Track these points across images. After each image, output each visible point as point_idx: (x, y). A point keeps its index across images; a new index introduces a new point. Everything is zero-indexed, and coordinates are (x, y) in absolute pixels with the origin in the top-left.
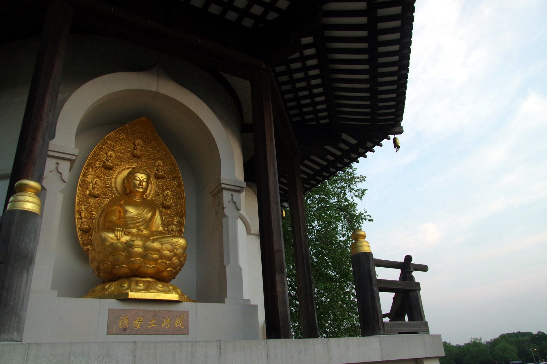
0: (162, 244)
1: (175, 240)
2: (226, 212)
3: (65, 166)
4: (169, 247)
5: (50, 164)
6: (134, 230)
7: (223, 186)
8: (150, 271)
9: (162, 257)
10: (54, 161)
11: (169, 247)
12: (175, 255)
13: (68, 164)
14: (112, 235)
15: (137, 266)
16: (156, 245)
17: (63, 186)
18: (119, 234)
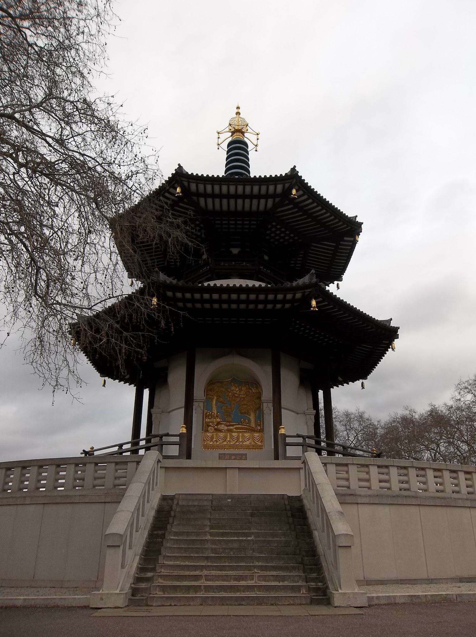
3: (201, 404)
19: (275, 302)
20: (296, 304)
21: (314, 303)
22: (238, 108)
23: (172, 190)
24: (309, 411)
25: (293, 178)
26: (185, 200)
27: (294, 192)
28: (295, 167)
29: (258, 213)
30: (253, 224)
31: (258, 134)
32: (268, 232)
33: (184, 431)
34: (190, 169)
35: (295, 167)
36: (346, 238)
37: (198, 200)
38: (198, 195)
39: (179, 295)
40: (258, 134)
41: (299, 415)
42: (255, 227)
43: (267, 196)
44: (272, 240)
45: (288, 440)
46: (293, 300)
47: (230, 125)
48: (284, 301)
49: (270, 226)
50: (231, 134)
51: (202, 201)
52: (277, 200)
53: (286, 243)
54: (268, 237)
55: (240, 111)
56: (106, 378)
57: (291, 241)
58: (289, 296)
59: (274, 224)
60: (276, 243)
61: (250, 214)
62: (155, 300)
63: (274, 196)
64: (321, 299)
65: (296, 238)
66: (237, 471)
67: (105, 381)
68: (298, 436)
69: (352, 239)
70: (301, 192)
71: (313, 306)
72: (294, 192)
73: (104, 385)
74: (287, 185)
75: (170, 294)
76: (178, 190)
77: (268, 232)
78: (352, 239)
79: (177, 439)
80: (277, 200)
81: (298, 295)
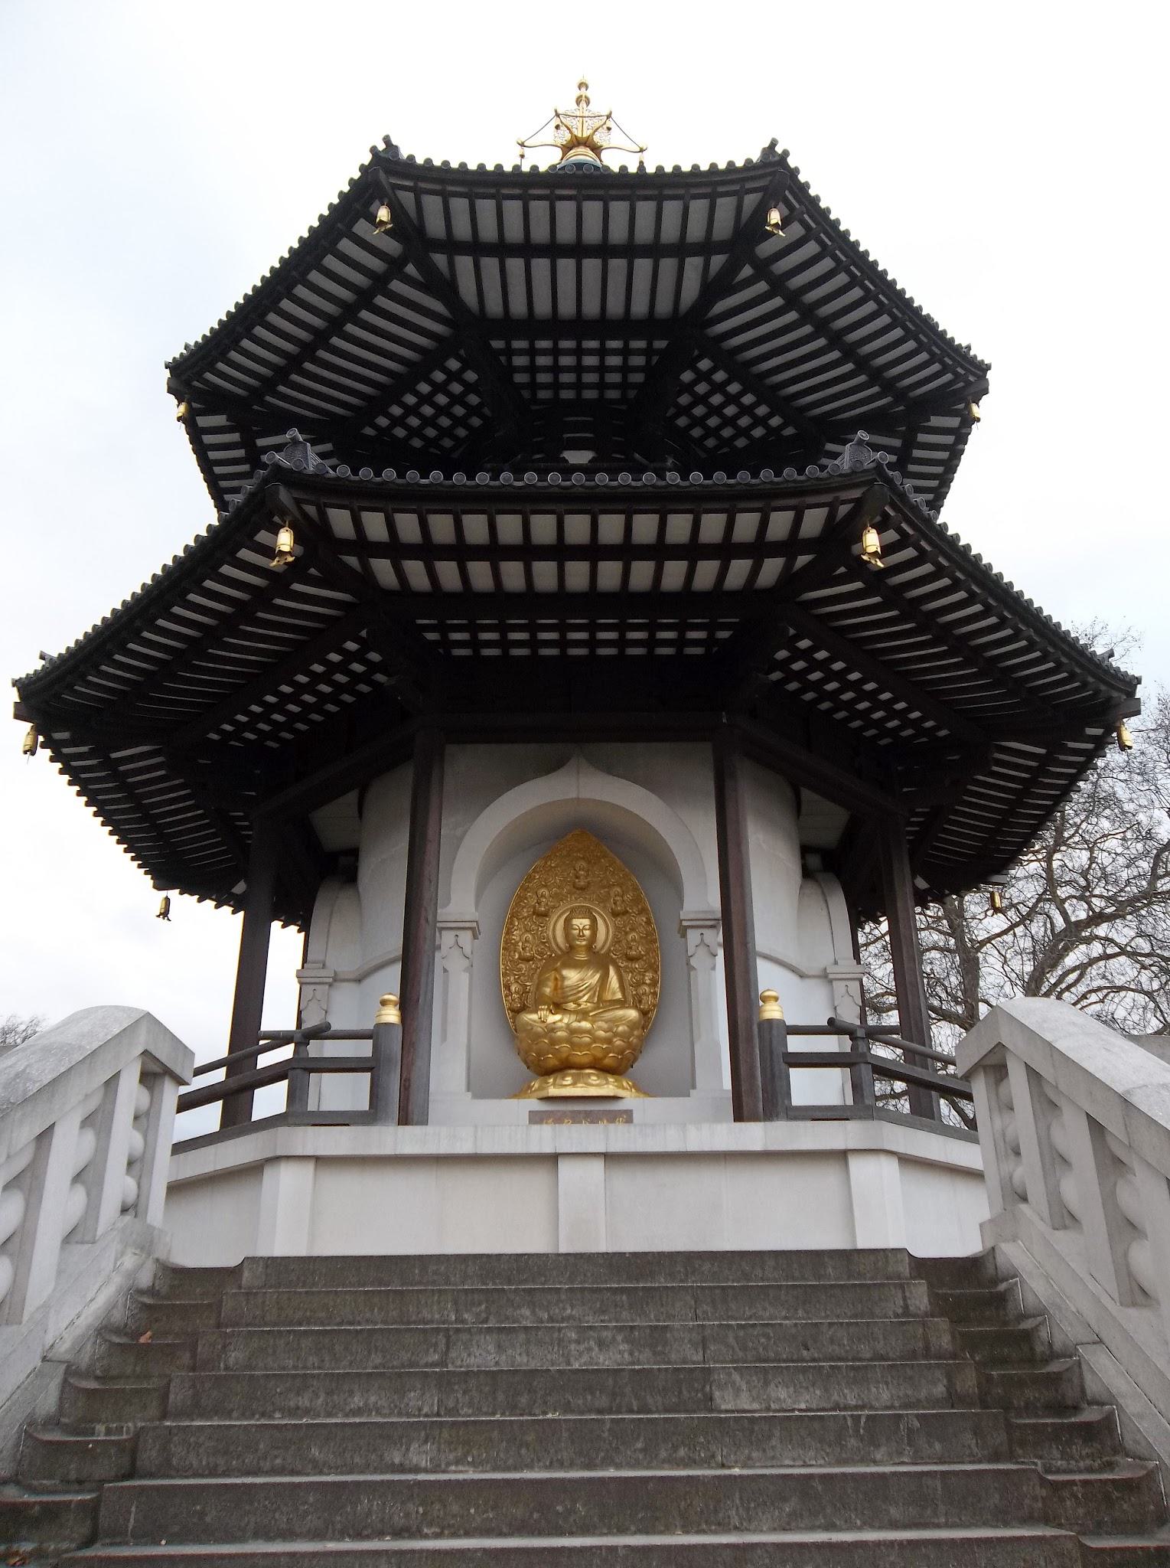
0: (593, 1022)
1: (620, 1013)
2: (693, 962)
3: (466, 938)
4: (605, 1026)
5: (447, 939)
6: (571, 1006)
7: (685, 923)
8: (585, 1060)
9: (595, 1039)
10: (453, 933)
11: (605, 1026)
12: (616, 1034)
13: (469, 933)
14: (534, 1017)
15: (564, 1055)
16: (585, 1025)
17: (466, 963)
18: (542, 1013)
19: (726, 550)
20: (802, 560)
21: (872, 540)
22: (582, 85)
23: (361, 227)
24: (836, 969)
25: (773, 177)
26: (410, 269)
27: (775, 217)
28: (774, 143)
29: (650, 326)
30: (636, 369)
31: (642, 150)
32: (684, 400)
33: (392, 1015)
34: (423, 146)
35: (774, 143)
36: (936, 421)
37: (451, 265)
38: (451, 246)
39: (375, 525)
40: (642, 150)
41: (807, 981)
42: (638, 378)
43: (681, 250)
44: (696, 432)
45: (796, 1044)
46: (791, 546)
47: (558, 115)
48: (759, 549)
49: (687, 376)
50: (559, 153)
51: (464, 264)
52: (718, 261)
53: (741, 443)
54: (682, 421)
55: (588, 93)
56: (174, 894)
57: (758, 432)
58: (780, 524)
59: (705, 364)
60: (711, 443)
61: (627, 327)
62: (285, 540)
63: (707, 248)
64: (892, 536)
65: (775, 421)
66: (597, 1167)
67: (167, 900)
68: (834, 1027)
69: (954, 422)
70: (796, 230)
71: (871, 550)
72: (775, 217)
73: (165, 914)
74: (751, 201)
75: (340, 521)
76: (383, 214)
77: (684, 400)
78: (954, 422)
79: (364, 1049)
80: (718, 261)
81: (814, 521)
